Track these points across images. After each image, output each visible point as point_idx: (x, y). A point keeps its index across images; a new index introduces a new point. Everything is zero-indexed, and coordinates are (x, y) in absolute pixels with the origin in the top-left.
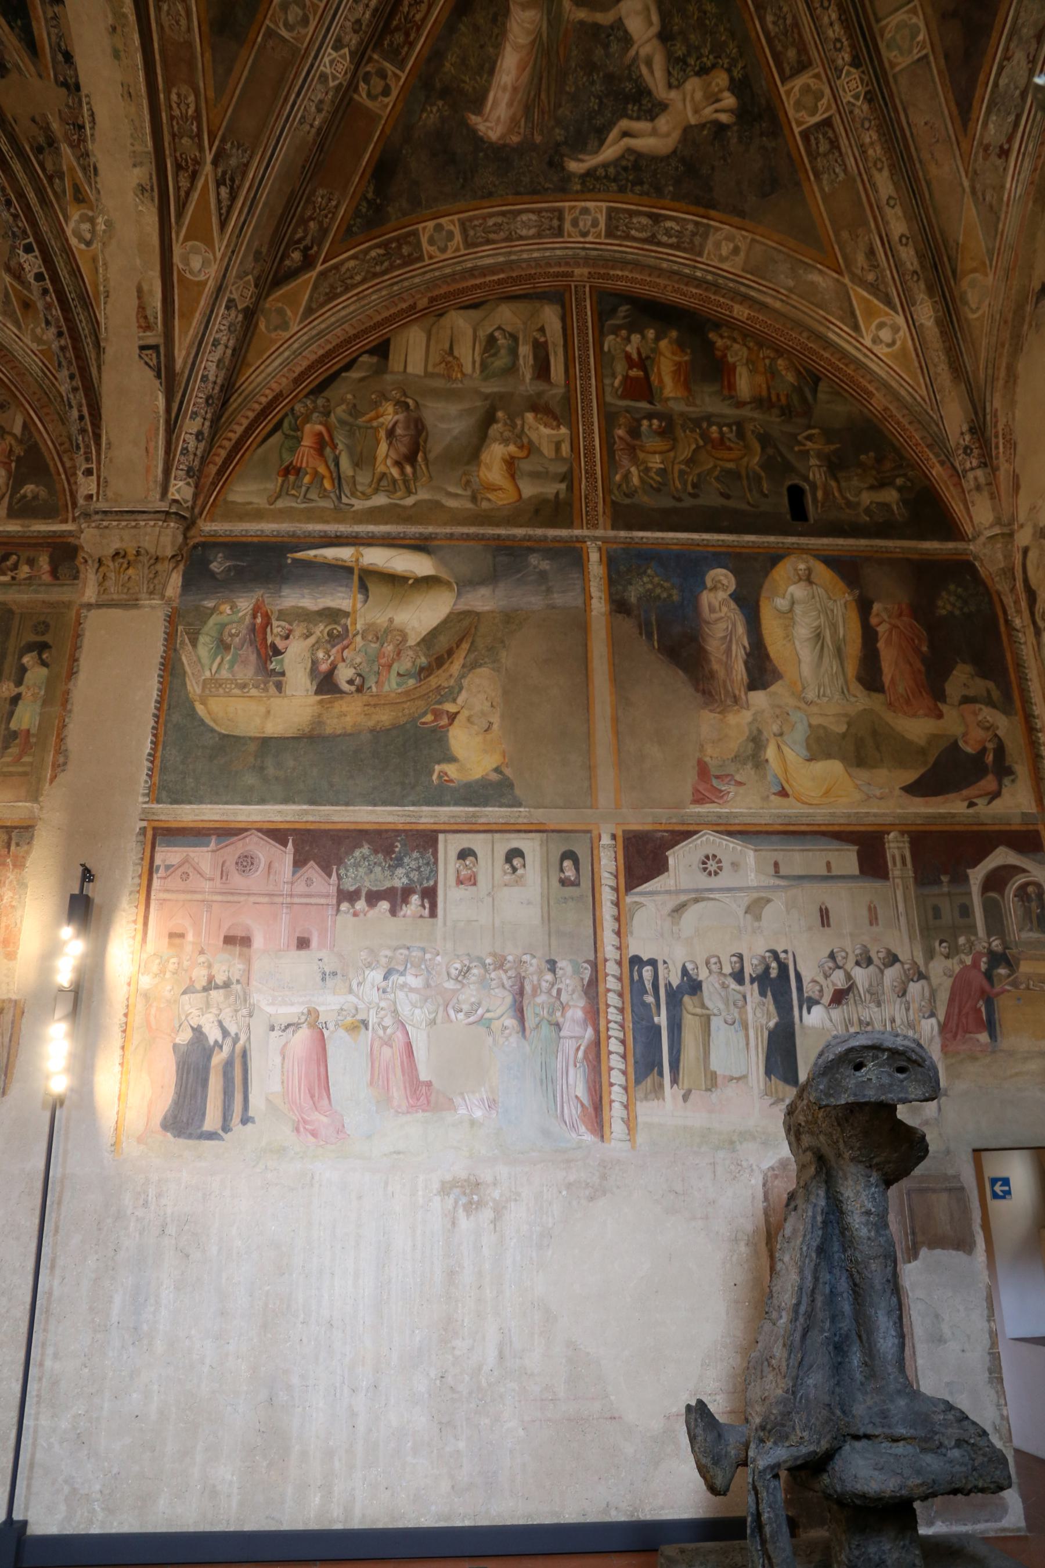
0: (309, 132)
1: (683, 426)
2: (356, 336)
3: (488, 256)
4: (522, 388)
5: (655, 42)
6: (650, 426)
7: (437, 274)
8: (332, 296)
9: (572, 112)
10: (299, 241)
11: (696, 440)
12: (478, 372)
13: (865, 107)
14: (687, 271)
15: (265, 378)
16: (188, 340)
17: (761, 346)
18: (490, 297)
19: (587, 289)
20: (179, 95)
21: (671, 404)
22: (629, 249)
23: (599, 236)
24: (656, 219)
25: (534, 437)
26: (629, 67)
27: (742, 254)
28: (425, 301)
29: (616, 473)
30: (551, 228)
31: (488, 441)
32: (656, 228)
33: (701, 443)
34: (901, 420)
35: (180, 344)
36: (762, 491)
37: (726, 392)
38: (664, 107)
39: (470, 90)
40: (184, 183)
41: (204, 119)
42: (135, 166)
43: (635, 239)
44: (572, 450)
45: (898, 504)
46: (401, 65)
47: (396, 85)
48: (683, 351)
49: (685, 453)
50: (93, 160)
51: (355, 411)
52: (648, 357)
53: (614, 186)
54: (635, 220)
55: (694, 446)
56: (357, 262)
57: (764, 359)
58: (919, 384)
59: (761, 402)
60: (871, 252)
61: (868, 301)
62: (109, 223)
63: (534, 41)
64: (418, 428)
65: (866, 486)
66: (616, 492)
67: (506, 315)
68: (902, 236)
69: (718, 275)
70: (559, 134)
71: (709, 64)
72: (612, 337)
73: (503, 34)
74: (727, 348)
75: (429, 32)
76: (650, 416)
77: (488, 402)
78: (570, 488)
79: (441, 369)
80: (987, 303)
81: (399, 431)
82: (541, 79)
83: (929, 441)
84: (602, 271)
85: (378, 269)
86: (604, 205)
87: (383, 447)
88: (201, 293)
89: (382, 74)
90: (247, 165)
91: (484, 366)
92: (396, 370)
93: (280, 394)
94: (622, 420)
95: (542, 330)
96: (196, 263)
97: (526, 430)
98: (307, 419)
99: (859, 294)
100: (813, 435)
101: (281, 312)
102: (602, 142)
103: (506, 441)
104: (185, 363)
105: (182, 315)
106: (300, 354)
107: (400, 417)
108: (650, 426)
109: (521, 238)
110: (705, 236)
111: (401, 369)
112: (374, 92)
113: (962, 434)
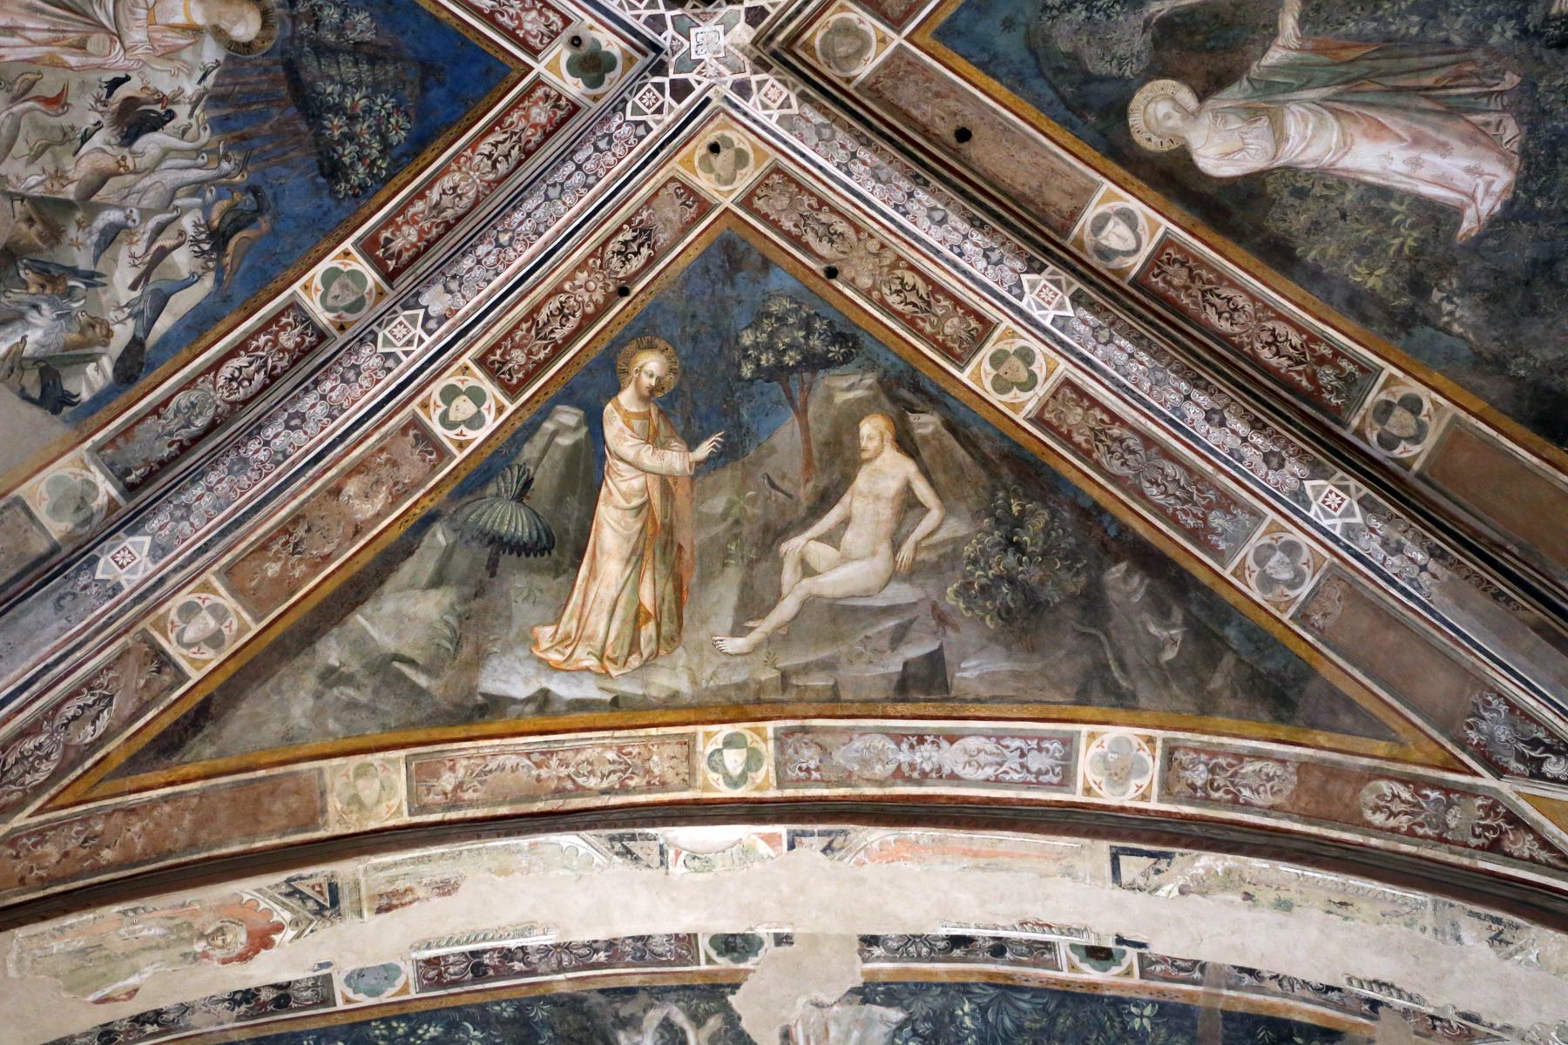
0: (1434, 576)
9: (1458, 14)
20: (1377, 809)
39: (1415, 234)
40: (1524, 845)
41: (1420, 771)
46: (1370, 372)
47: (1403, 384)
50: (1450, 1014)
63: (1334, 111)
70: (1502, 34)
73: (1322, 175)
75: (1319, 319)
82: (1398, 90)
89: (1384, 410)
90: (1513, 707)
112: (1411, 432)
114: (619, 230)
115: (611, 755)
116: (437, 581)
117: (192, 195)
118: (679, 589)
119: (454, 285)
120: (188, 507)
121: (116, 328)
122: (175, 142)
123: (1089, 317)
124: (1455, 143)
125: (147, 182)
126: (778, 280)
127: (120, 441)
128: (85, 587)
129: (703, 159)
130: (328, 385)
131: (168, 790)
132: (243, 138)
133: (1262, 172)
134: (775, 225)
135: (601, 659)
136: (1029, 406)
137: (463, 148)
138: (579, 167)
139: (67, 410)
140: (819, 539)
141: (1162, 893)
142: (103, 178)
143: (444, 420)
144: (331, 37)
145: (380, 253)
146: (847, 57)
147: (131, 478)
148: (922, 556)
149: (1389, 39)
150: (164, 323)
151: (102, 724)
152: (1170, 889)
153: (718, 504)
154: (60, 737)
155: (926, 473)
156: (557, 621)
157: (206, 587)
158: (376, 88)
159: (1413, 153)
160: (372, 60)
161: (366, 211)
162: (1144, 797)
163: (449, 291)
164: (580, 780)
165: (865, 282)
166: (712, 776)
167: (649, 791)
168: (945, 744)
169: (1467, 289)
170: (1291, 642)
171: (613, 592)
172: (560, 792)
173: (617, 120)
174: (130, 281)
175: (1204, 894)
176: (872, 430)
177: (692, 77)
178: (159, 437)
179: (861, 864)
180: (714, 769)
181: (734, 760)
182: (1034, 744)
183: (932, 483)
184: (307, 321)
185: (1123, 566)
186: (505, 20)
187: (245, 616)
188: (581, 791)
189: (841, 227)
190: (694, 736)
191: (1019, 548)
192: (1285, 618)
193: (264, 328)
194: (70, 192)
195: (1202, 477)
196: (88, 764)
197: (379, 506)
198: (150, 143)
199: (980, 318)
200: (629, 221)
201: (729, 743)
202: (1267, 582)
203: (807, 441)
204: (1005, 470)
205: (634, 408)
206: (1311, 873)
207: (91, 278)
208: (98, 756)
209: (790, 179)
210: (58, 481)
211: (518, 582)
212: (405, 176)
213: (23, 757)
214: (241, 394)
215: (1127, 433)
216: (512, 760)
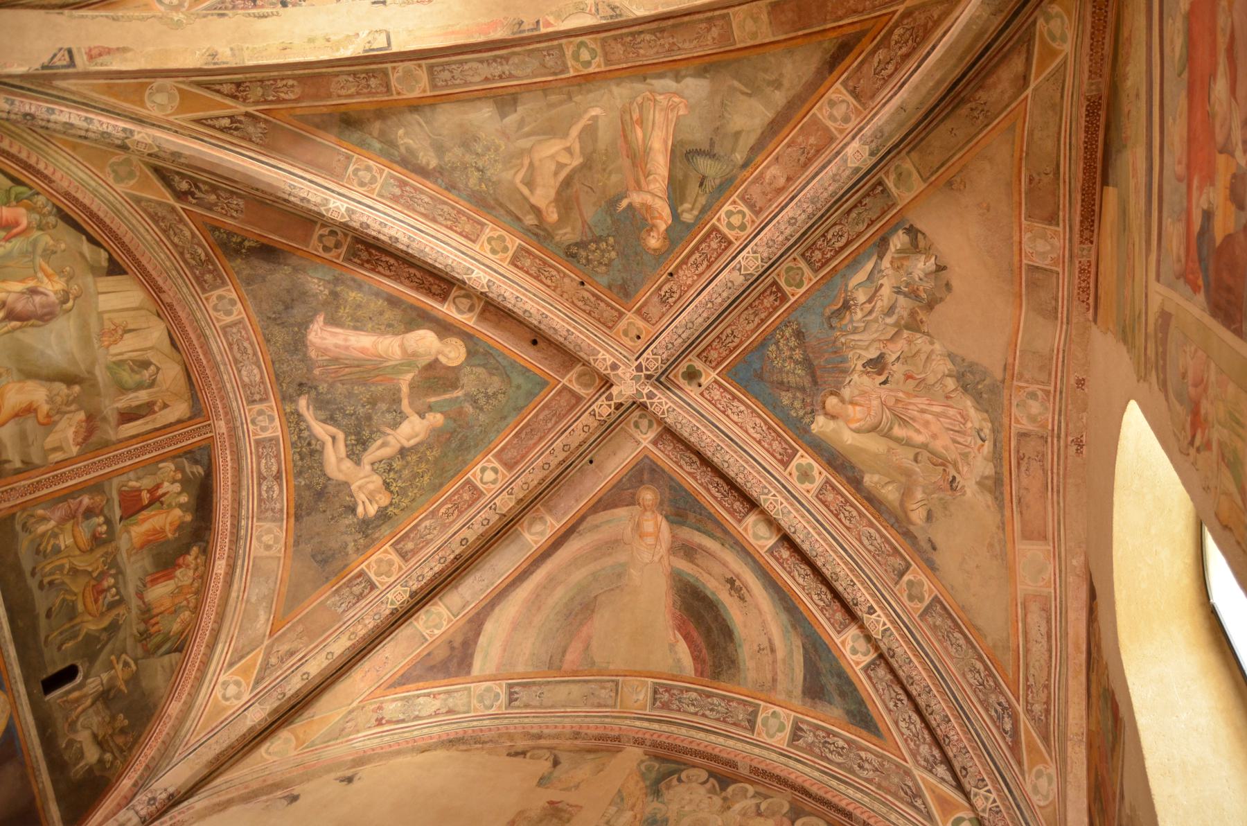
1: (106, 553)
2: (123, 244)
3: (219, 347)
4: (107, 402)
5: (398, 446)
6: (99, 525)
7: (194, 306)
8: (155, 218)
10: (197, 187)
11: (97, 568)
12: (114, 359)
13: (388, 612)
14: (244, 512)
15: (64, 165)
16: (86, 92)
17: (197, 593)
18: (184, 355)
19: (209, 435)
20: (293, 86)
21: (125, 536)
22: (249, 462)
23: (255, 434)
24: (278, 477)
25: (62, 424)
26: (379, 431)
27: (267, 553)
28: (169, 301)
29: (44, 509)
30: (252, 394)
31: (48, 383)
32: (271, 479)
33: (95, 575)
34: (164, 733)
35: (81, 85)
36: (62, 644)
37: (148, 579)
38: (358, 462)
40: (226, 88)
42: (232, 49)
43: (259, 464)
44: (57, 463)
45: (86, 765)
48: (175, 531)
49: (81, 564)
50: (230, 13)
51: (48, 253)
52: (162, 503)
53: (295, 438)
54: (273, 460)
55: (90, 569)
56: (189, 238)
57: (186, 599)
58: (198, 734)
59: (147, 613)
60: (292, 653)
61: (255, 665)
62: (179, 25)
63: (381, 356)
64: (45, 316)
65: (96, 732)
66: (25, 515)
67: (171, 373)
68: (308, 673)
69: (246, 539)
70: (323, 388)
71: (392, 488)
72: (173, 467)
73: (382, 334)
74: (188, 566)
76: (108, 522)
77: (86, 375)
78: (18, 472)
79: (108, 325)
80: (275, 759)
81: (38, 299)
82: (358, 366)
83: (152, 765)
84: (227, 444)
85: (188, 256)
86: (279, 433)
87: (18, 287)
88: (133, 102)
90: (250, 140)
91: (120, 364)
92: (99, 285)
93: (51, 181)
94: (98, 499)
95: (165, 406)
96: (161, 98)
97: (67, 416)
98: (31, 209)
99: (258, 656)
100: (130, 666)
101: (131, 175)
102: (324, 421)
103: (51, 400)
104: (64, 90)
105: (110, 86)
106: (95, 196)
107: (53, 298)
108: (99, 525)
109: (239, 371)
110: (274, 520)
111: (100, 290)
112: (324, 239)
113: (166, 790)
114: (675, 303)
115: (642, 52)
116: (737, 135)
117: (856, 328)
118: (625, 136)
119: (730, 284)
120: (834, 181)
121: (889, 265)
122: (863, 353)
123: (456, 275)
124: (333, 349)
125: (875, 335)
126: (604, 280)
127: (886, 208)
128: (872, 141)
129: (642, 333)
130: (781, 238)
131: (841, 23)
132: (836, 352)
133: (407, 332)
134: (608, 305)
135: (655, 100)
136: (488, 231)
137: (746, 341)
138: (680, 336)
139: (907, 226)
140: (566, 165)
141: (367, 32)
142: (892, 339)
143: (744, 216)
144: (798, 394)
145: (779, 295)
146: (585, 375)
147: (880, 188)
148: (519, 161)
149: (365, 384)
150: (869, 266)
151: (876, 60)
152: (363, 35)
153: (614, 178)
154: (893, 53)
155: (525, 199)
156: (678, 118)
157: (841, 131)
158: (781, 371)
159: (348, 344)
160: (782, 383)
161: (785, 315)
162: (394, 68)
163: (732, 282)
164: (654, 38)
165: (566, 280)
166: (593, 46)
167: (621, 35)
168: (489, 76)
169: (315, 295)
170: (351, 147)
171: (655, 133)
172: (662, 30)
173: (665, 356)
174: (883, 288)
175: (348, 36)
176: (552, 216)
177: (635, 373)
178: (870, 209)
179: (505, 18)
180: (593, 49)
181: (585, 55)
182: (450, 83)
183: (521, 194)
184: (809, 263)
185: (431, 167)
186: (728, 396)
187: (820, 117)
188: (653, 32)
189: (580, 304)
190: (606, 65)
191: (478, 169)
192: (356, 156)
193: (828, 260)
194: (906, 333)
195: (408, 208)
196: (879, 38)
197: (768, 172)
198: (873, 354)
199: (516, 266)
200: (671, 306)
201: (588, 64)
202: (368, 168)
203: (580, 210)
204: (492, 202)
205: (658, 222)
206: (301, 59)
207: (898, 291)
208: (875, 42)
209: (604, 324)
210: (909, 190)
211: (699, 136)
212: (769, 330)
213: (906, 42)
214: (837, 228)
215: (444, 222)
216: (686, 45)
